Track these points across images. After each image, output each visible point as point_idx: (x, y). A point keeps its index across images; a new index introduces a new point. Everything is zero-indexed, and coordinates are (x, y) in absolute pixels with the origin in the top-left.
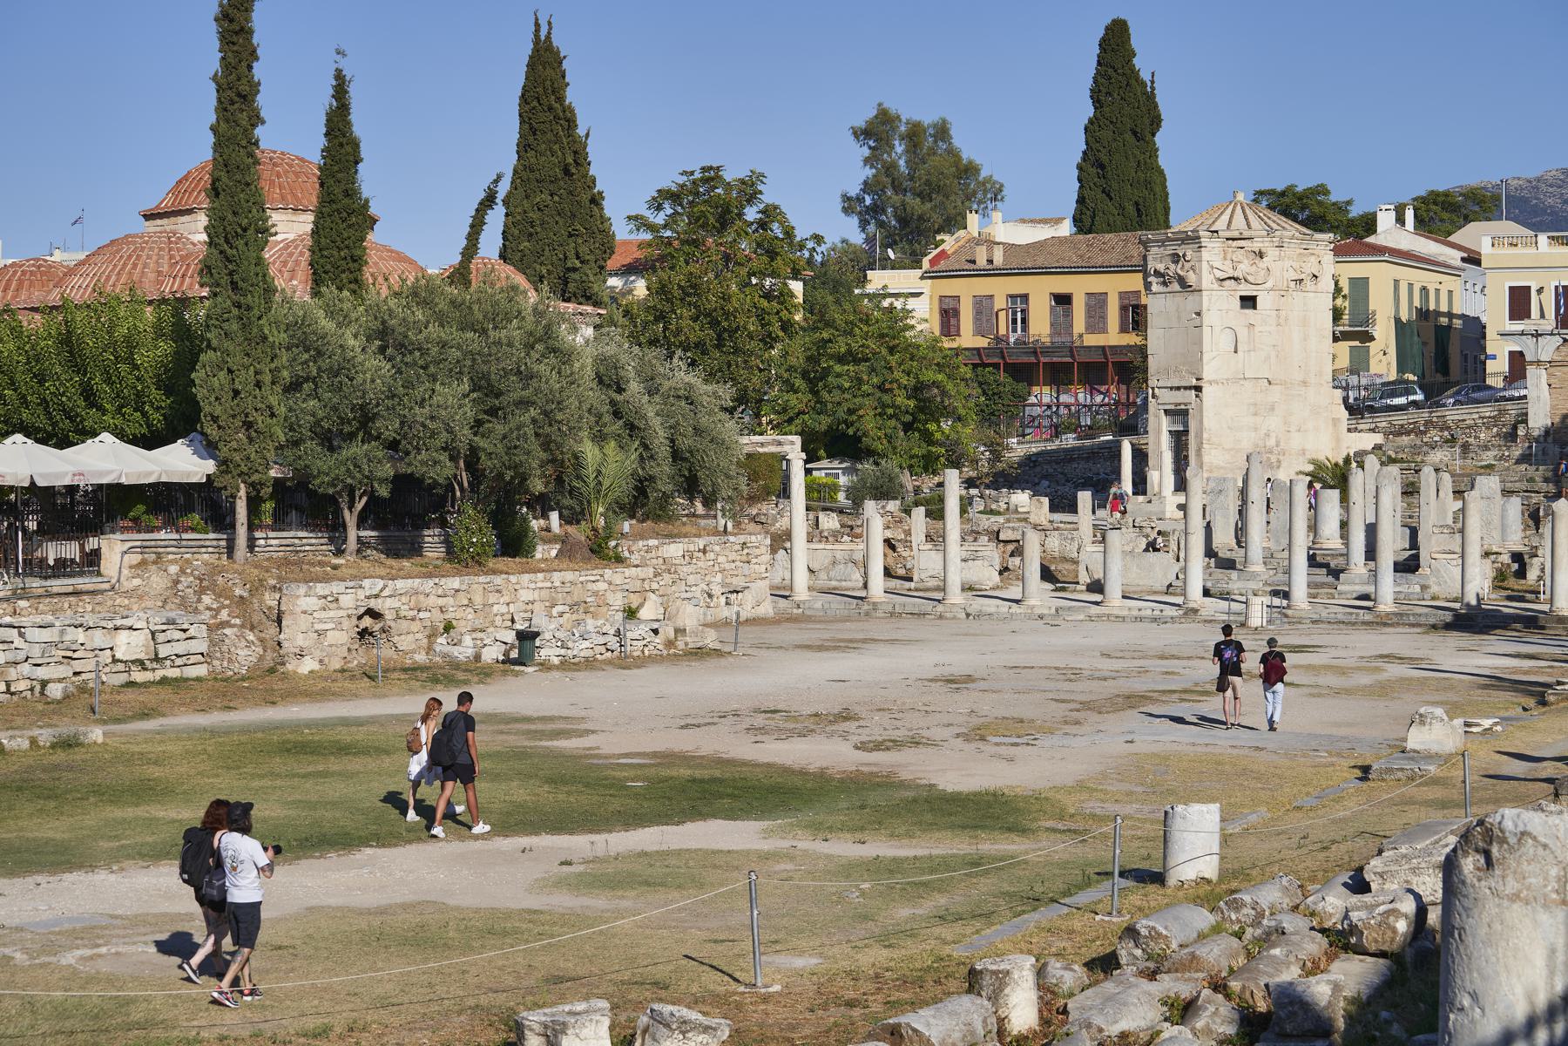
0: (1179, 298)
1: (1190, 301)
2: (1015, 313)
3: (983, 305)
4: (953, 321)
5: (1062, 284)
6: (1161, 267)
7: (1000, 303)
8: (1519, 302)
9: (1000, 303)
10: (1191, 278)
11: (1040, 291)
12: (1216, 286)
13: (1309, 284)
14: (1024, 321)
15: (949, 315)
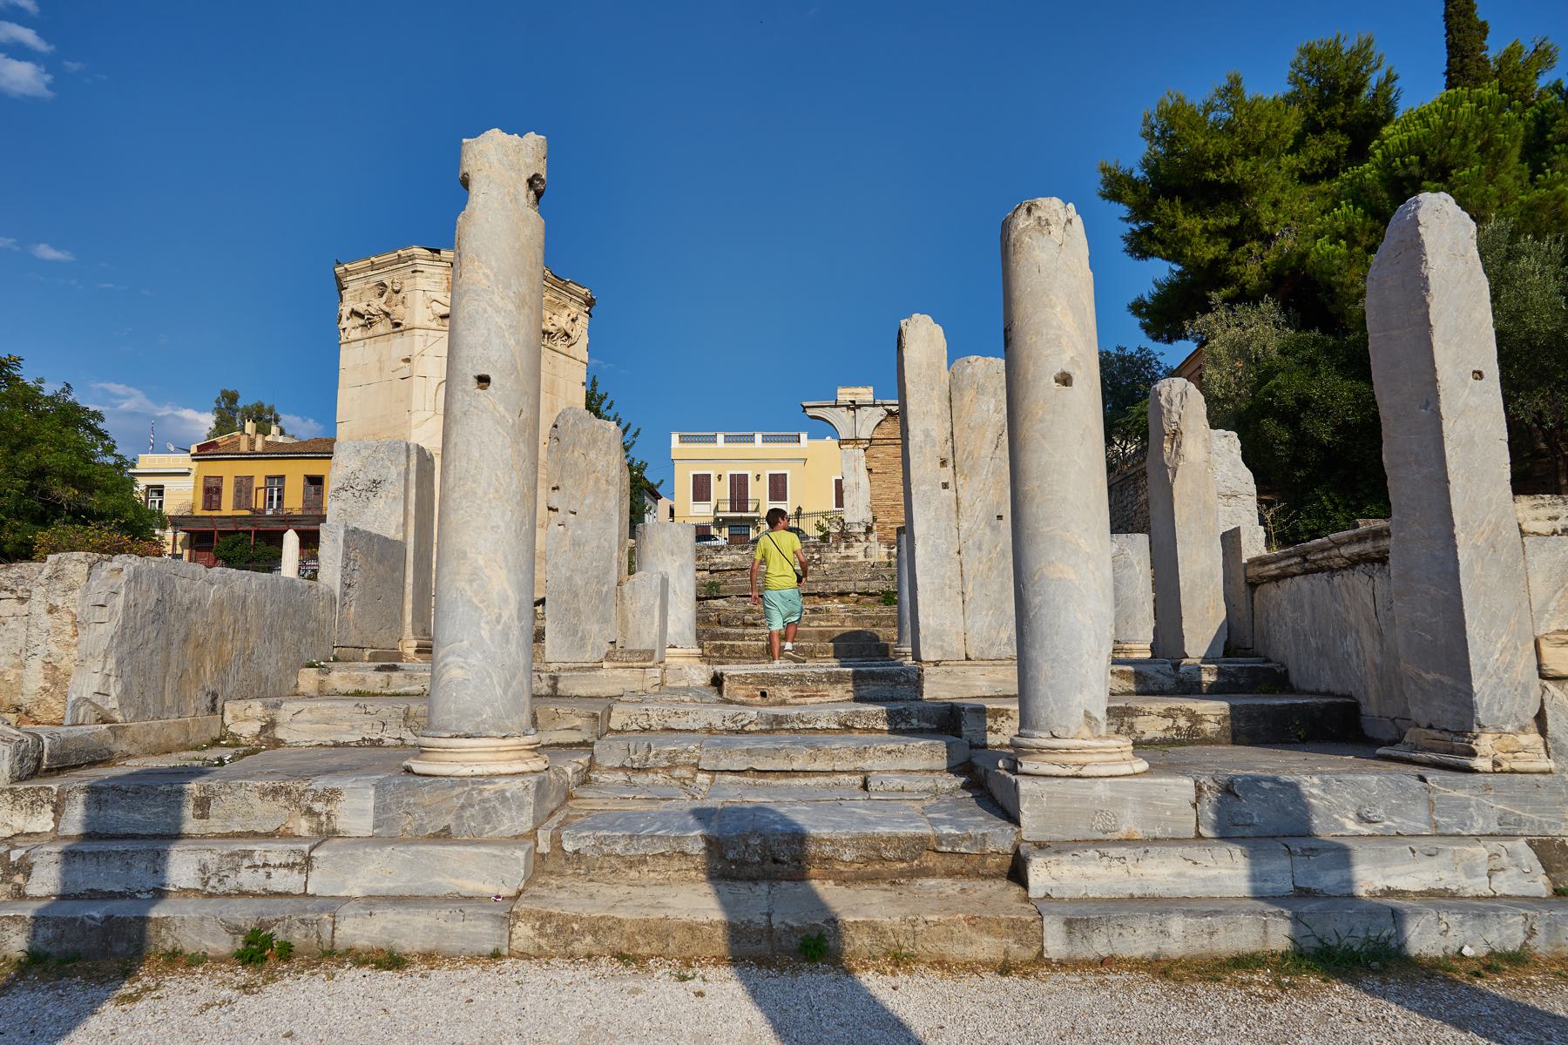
0: (381, 344)
1: (399, 346)
2: (272, 492)
3: (243, 486)
4: (215, 498)
5: (314, 468)
6: (361, 308)
7: (259, 482)
8: (701, 488)
9: (259, 482)
10: (398, 312)
11: (295, 473)
12: (434, 325)
13: (560, 344)
14: (279, 498)
15: (212, 492)
